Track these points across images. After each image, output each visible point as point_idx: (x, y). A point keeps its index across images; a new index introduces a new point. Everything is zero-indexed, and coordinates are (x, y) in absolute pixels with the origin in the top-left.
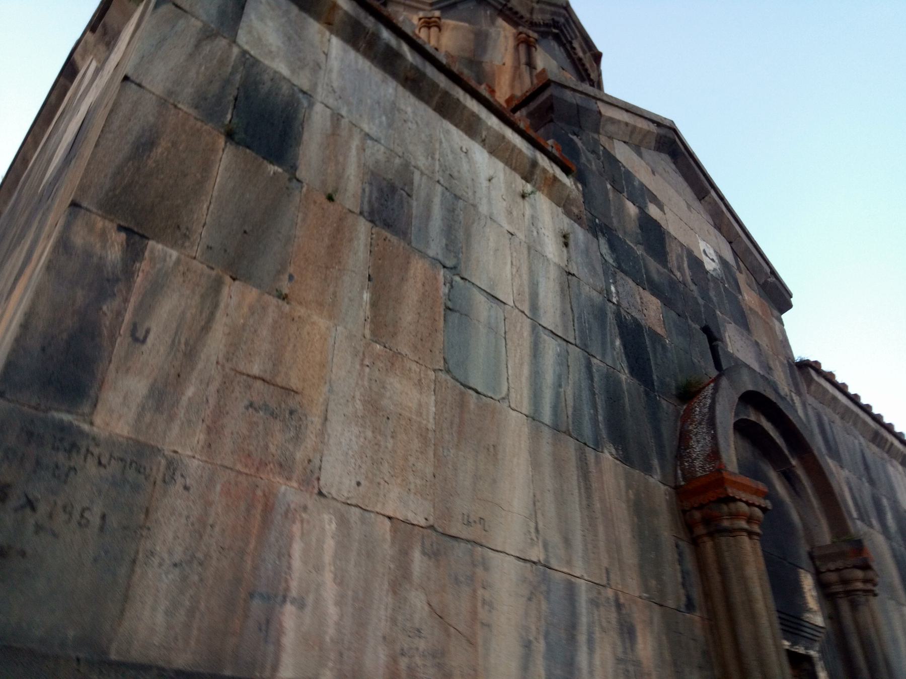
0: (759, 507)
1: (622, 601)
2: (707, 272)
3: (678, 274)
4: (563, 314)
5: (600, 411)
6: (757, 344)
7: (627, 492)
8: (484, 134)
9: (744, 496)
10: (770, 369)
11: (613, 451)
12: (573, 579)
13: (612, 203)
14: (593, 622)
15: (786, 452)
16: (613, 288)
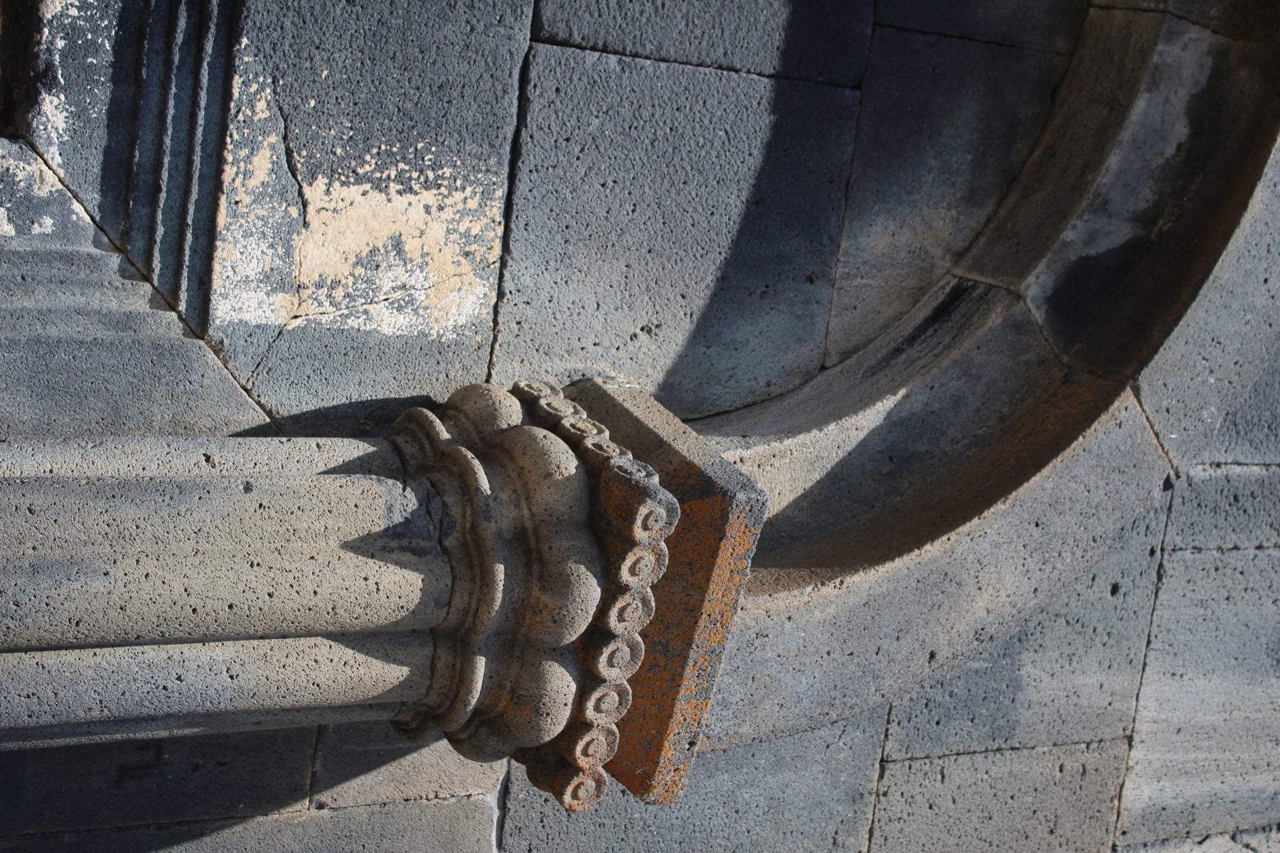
15: (1077, 236)
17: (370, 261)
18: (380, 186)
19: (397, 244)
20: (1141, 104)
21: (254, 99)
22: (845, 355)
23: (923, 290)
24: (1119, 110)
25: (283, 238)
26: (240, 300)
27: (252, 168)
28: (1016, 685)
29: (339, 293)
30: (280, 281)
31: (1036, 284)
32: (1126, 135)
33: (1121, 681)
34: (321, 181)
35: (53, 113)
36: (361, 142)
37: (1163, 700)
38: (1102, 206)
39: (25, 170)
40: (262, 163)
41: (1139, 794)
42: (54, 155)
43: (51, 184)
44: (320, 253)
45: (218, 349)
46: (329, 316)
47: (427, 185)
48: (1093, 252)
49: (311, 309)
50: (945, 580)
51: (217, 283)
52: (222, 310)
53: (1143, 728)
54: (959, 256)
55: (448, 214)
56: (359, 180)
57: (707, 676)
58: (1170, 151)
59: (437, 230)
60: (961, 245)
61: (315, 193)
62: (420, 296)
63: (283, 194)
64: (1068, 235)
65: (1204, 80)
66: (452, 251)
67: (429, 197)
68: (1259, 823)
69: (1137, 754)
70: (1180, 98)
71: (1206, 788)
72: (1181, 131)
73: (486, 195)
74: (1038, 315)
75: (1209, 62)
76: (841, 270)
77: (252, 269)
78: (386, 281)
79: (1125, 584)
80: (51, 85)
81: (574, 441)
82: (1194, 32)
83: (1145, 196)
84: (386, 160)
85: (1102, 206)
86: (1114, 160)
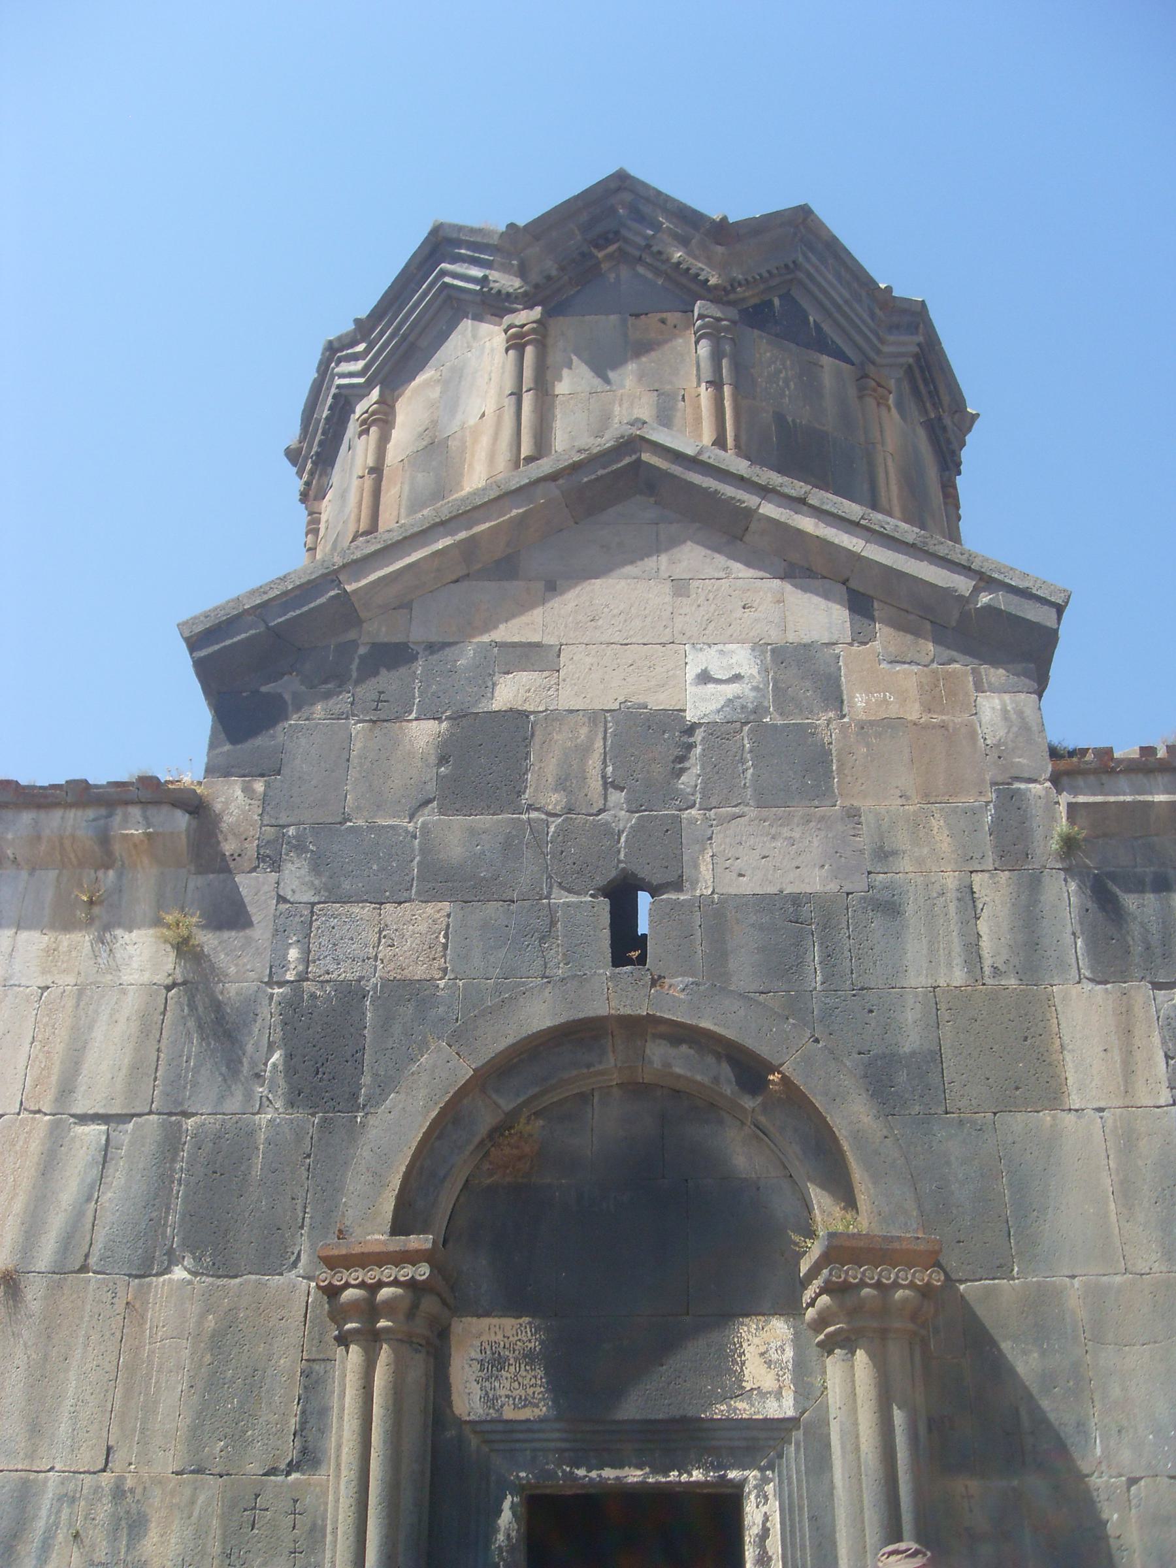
0: (395, 1283)
1: (129, 1483)
2: (691, 729)
3: (554, 800)
4: (135, 1068)
5: (178, 1204)
6: (853, 814)
7: (202, 1316)
8: (9, 852)
9: (357, 1275)
10: (884, 854)
11: (188, 1261)
12: (32, 1476)
13: (354, 761)
14: (57, 1525)
15: (728, 1089)
16: (293, 954)
17: (769, 1363)
18: (743, 1363)
19: (762, 1354)
20: (678, 1070)
21: (720, 1411)
22: (785, 1167)
23: (757, 1137)
24: (679, 1077)
25: (763, 1395)
26: (784, 1407)
27: (743, 1409)
28: (913, 1054)
29: (781, 1373)
30: (778, 1395)
31: (749, 1103)
32: (689, 1074)
33: (910, 1000)
34: (744, 1384)
35: (732, 1474)
36: (730, 1372)
37: (917, 979)
38: (716, 1079)
39: (752, 1482)
40: (741, 1405)
41: (959, 977)
42: (746, 1473)
43: (755, 1472)
44: (768, 1382)
45: (803, 1413)
46: (788, 1376)
47: (741, 1346)
48: (733, 1079)
49: (787, 1382)
50: (858, 1137)
51: (781, 1416)
52: (790, 1413)
53: (930, 982)
54: (743, 1123)
55: (750, 1337)
56: (742, 1370)
57: (891, 1239)
58: (692, 1052)
59: (756, 1341)
60: (739, 1123)
61: (748, 1386)
62: (779, 1343)
63: (750, 1397)
64: (729, 1092)
65: (664, 1042)
66: (763, 1334)
67: (745, 1345)
68: (971, 905)
69: (942, 983)
70: (672, 1051)
71: (956, 940)
72: (684, 1048)
73: (742, 1324)
74: (760, 1099)
75: (658, 1041)
76: (753, 1175)
77: (776, 1404)
78: (775, 1357)
79: (868, 1006)
80: (725, 1476)
81: (818, 1295)
82: (648, 1051)
83: (710, 1060)
84: (735, 1362)
85: (716, 1079)
86: (699, 1078)
